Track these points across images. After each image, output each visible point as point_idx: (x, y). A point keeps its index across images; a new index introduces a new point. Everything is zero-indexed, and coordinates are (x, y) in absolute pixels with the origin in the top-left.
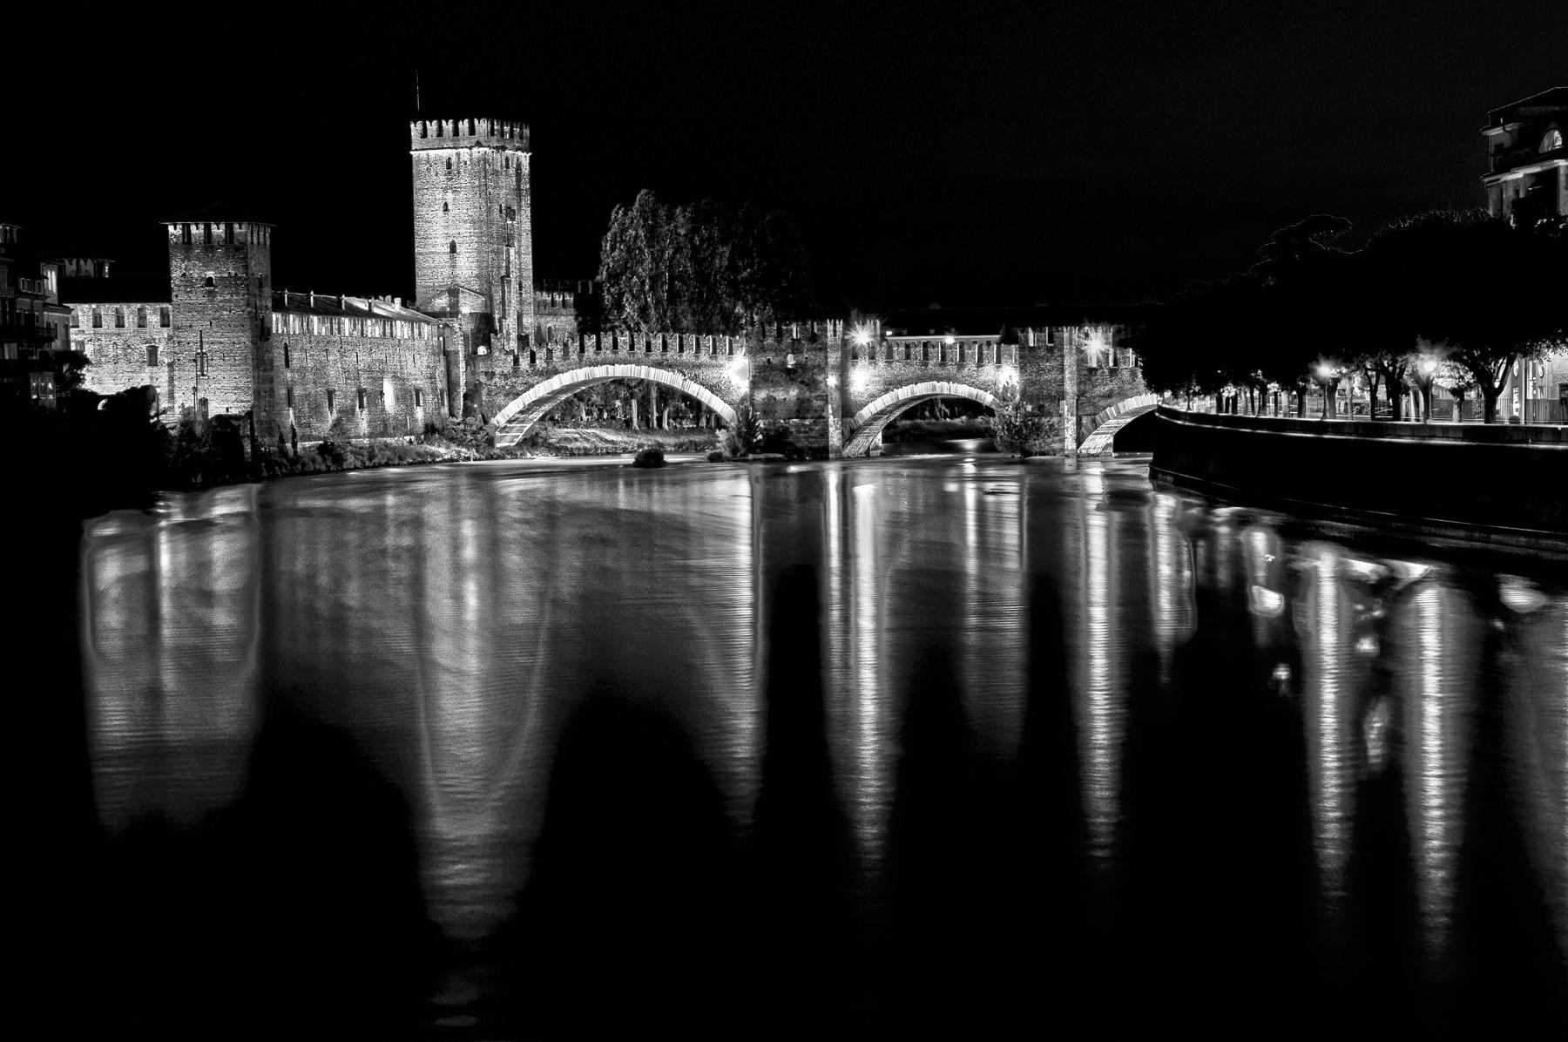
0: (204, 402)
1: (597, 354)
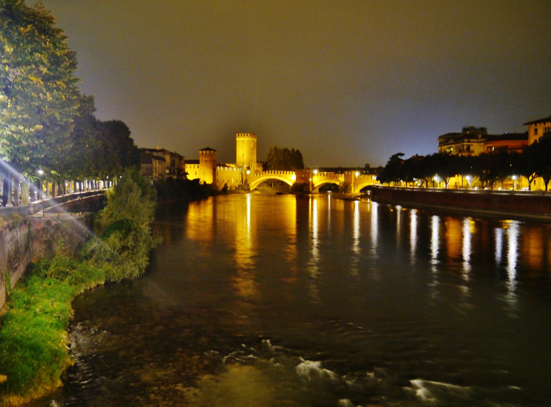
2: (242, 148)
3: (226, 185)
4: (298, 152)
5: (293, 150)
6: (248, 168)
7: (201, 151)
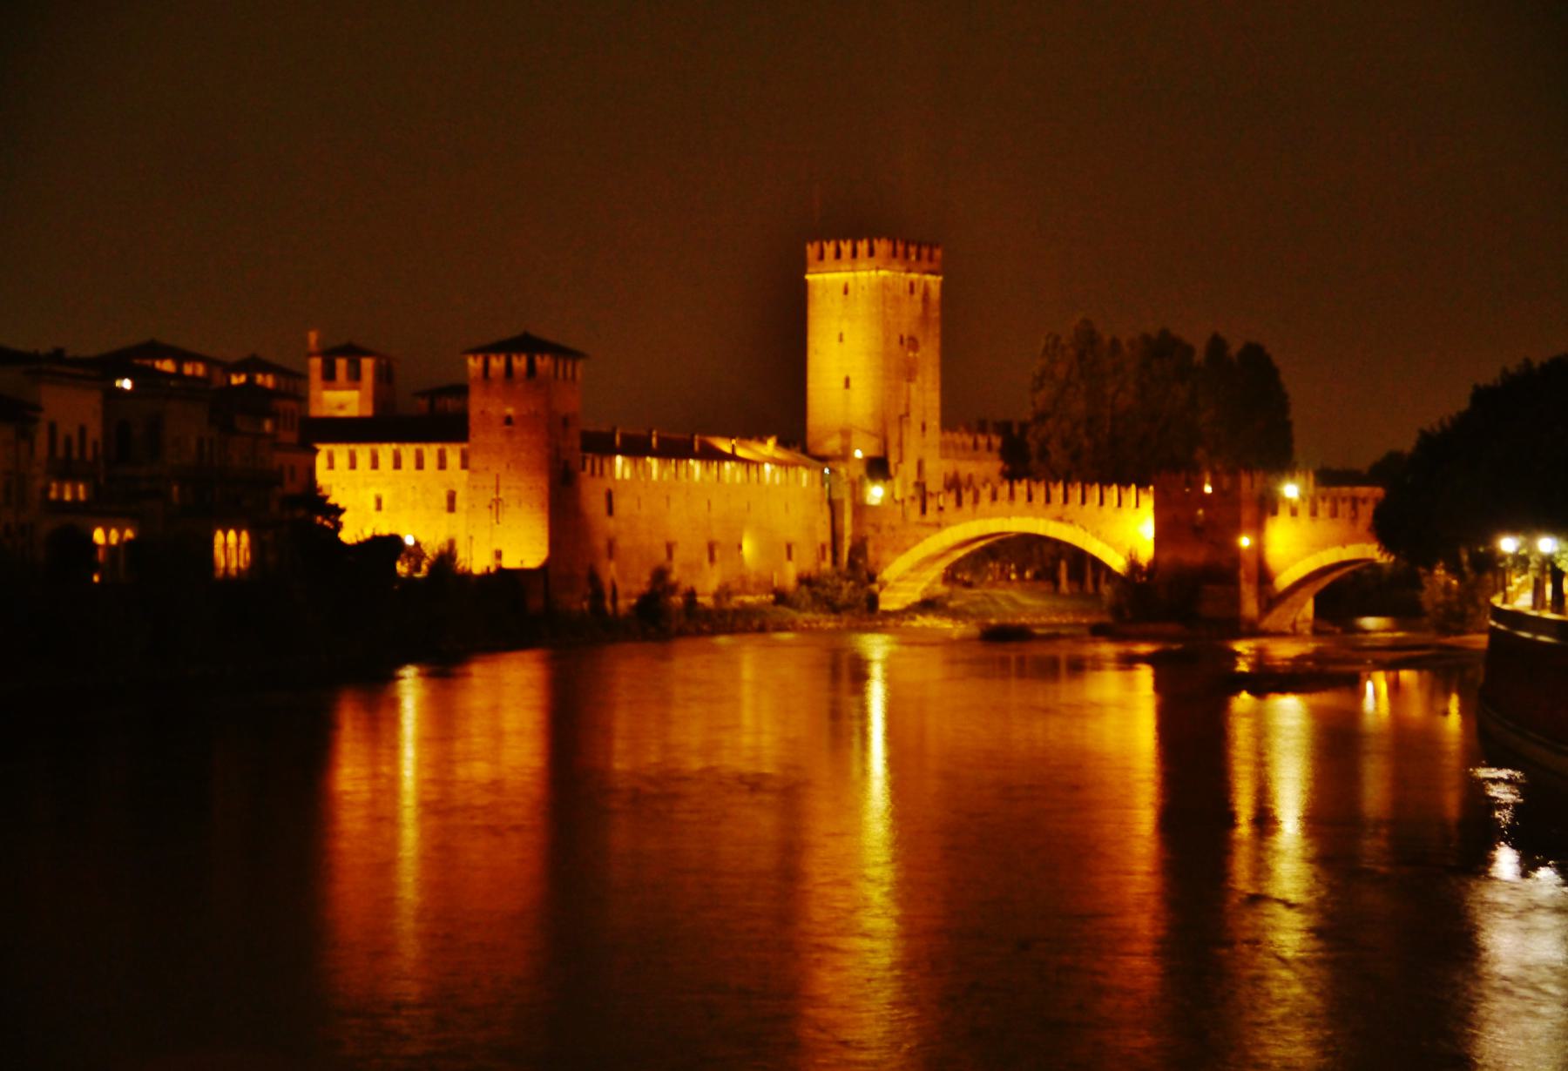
0: (499, 555)
2: (841, 339)
3: (660, 574)
4: (1256, 356)
5: (1217, 345)
6: (878, 468)
7: (480, 359)
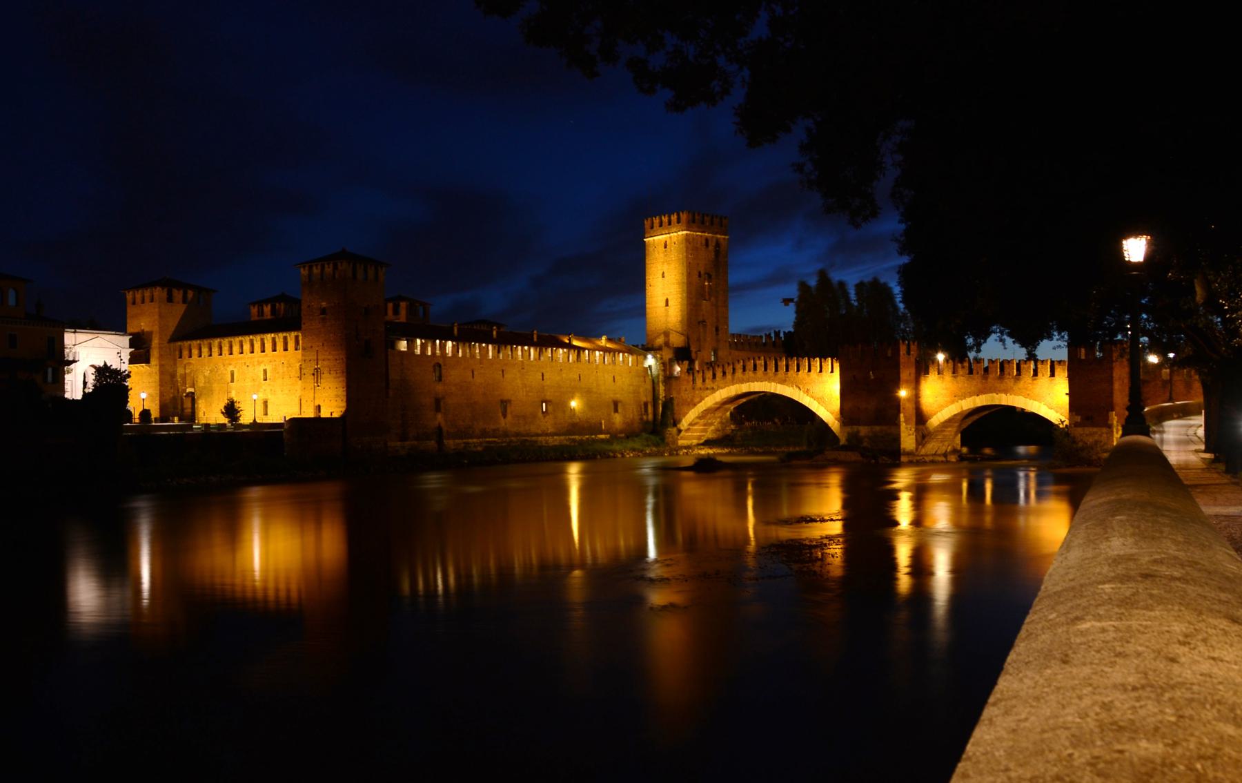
0: (319, 408)
1: (744, 374)
